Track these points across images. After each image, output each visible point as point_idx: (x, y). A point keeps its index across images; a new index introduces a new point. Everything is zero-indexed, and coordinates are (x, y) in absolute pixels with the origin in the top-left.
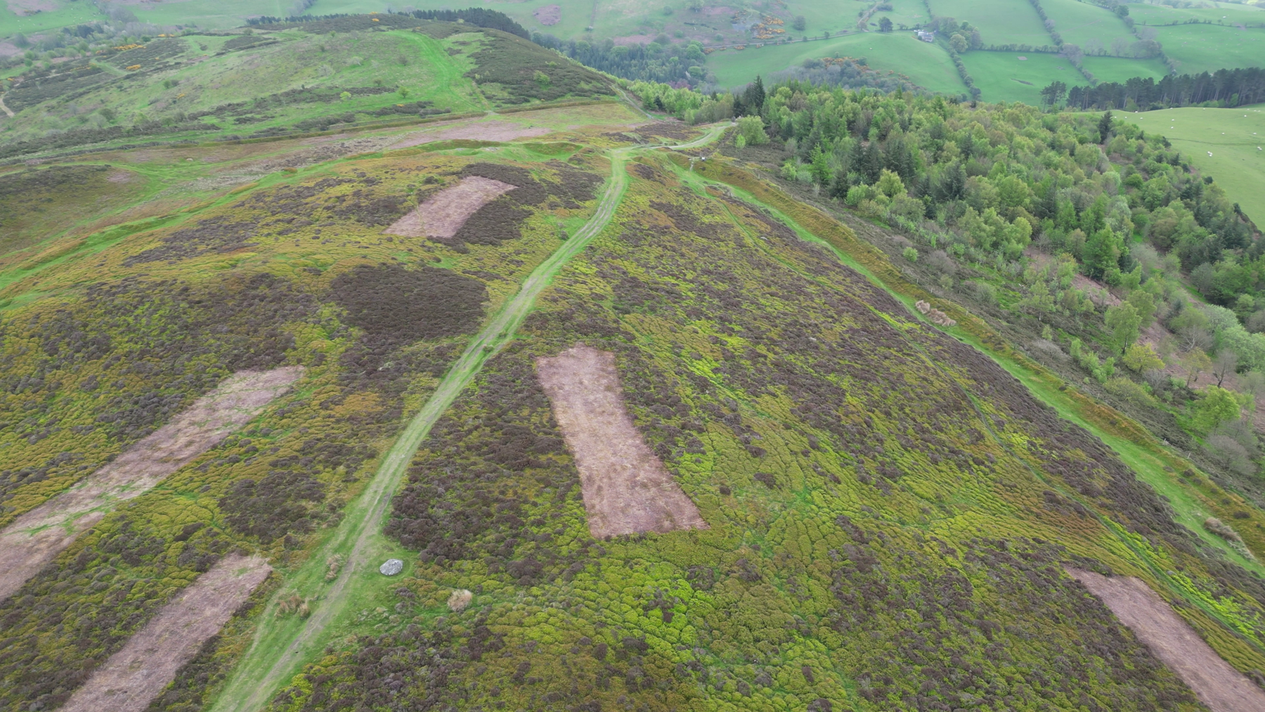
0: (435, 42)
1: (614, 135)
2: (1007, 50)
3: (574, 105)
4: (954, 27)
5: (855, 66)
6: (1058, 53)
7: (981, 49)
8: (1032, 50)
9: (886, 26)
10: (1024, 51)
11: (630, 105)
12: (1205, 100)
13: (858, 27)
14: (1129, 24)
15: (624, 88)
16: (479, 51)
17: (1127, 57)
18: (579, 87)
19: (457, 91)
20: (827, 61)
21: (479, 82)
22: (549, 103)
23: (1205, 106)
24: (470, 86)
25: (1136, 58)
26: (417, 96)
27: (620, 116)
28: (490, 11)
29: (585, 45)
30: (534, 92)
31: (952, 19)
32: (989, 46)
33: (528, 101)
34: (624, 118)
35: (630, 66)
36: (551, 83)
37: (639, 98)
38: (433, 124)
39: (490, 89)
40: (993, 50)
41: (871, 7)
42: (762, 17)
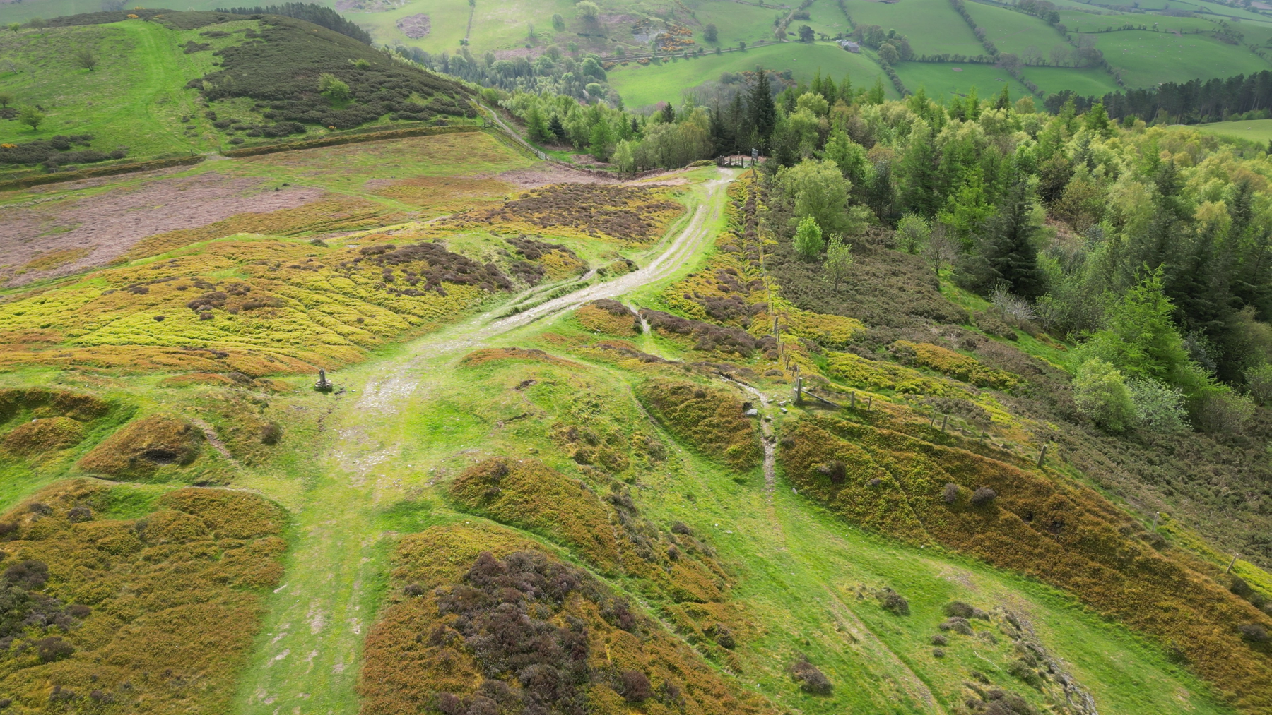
0: (169, 32)
1: (408, 256)
2: (940, 60)
3: (393, 136)
4: (880, 36)
5: (779, 80)
6: (993, 64)
7: (911, 60)
8: (966, 60)
9: (807, 35)
10: (957, 62)
11: (504, 134)
12: (1248, 110)
13: (776, 37)
14: (1062, 31)
15: (493, 103)
16: (238, 45)
17: (1066, 67)
18: (407, 102)
19: (160, 114)
20: (746, 74)
21: (212, 96)
22: (347, 134)
23: (1249, 118)
24: (191, 103)
25: (1077, 68)
26: (55, 123)
27: (484, 157)
28: (312, 5)
29: (460, 60)
30: (315, 113)
31: (878, 27)
32: (921, 57)
33: (302, 131)
34: (493, 160)
35: (516, 84)
36: (353, 95)
37: (520, 121)
38: (66, 185)
39: (223, 109)
40: (924, 61)
41: (786, 15)
42: (668, 27)
